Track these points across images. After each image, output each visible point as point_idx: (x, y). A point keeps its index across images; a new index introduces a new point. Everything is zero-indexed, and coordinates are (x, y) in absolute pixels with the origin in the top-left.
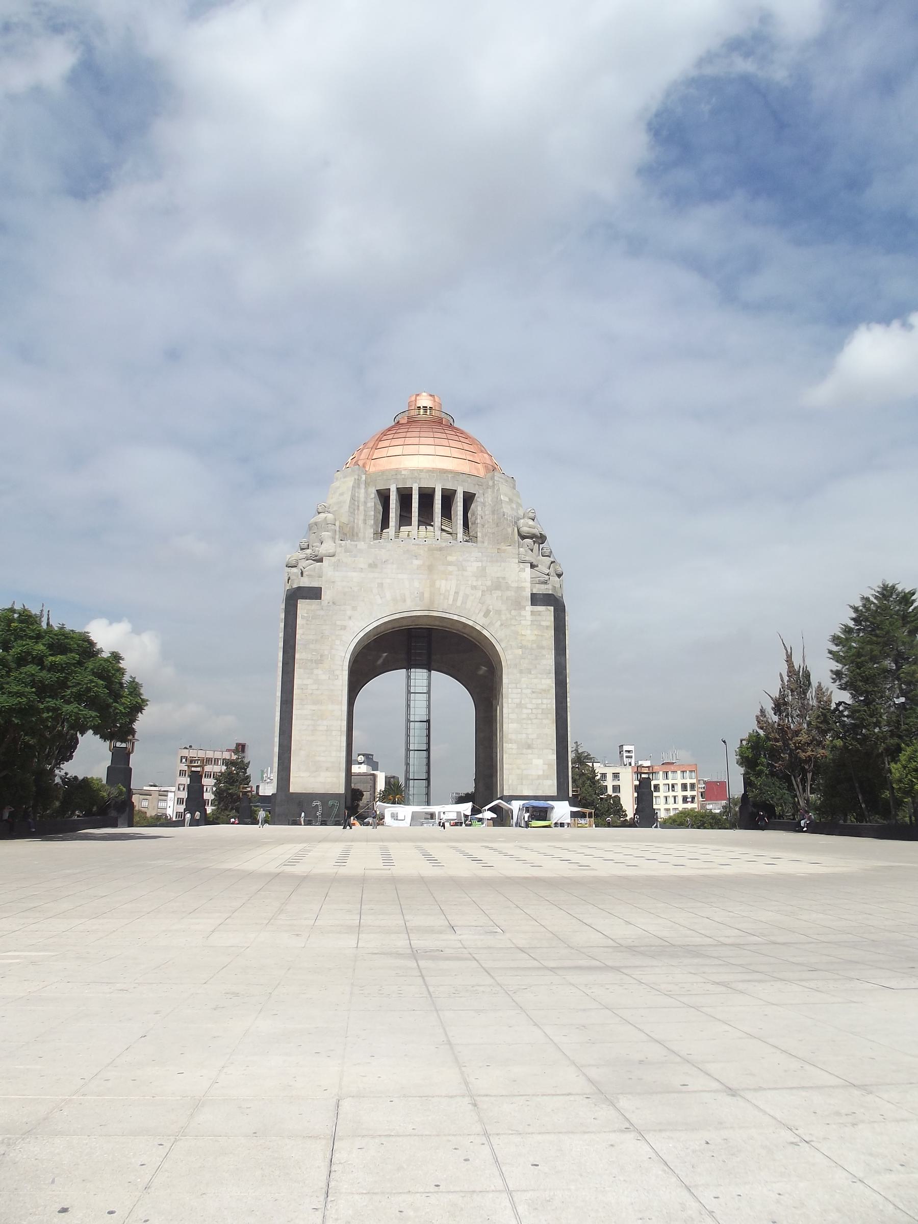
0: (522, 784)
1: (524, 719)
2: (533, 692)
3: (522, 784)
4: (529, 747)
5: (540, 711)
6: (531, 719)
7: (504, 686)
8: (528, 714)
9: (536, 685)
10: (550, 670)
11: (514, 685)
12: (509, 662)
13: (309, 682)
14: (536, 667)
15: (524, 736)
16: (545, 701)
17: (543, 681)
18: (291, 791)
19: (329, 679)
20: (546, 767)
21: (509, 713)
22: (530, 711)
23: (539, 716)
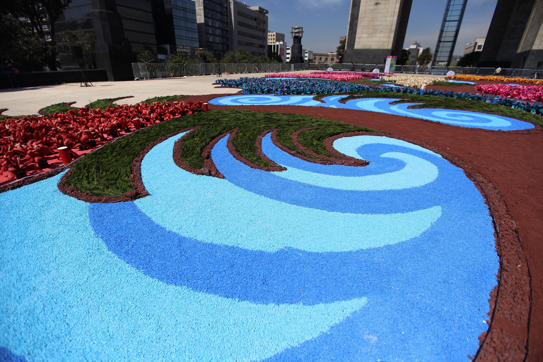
18: (356, 47)
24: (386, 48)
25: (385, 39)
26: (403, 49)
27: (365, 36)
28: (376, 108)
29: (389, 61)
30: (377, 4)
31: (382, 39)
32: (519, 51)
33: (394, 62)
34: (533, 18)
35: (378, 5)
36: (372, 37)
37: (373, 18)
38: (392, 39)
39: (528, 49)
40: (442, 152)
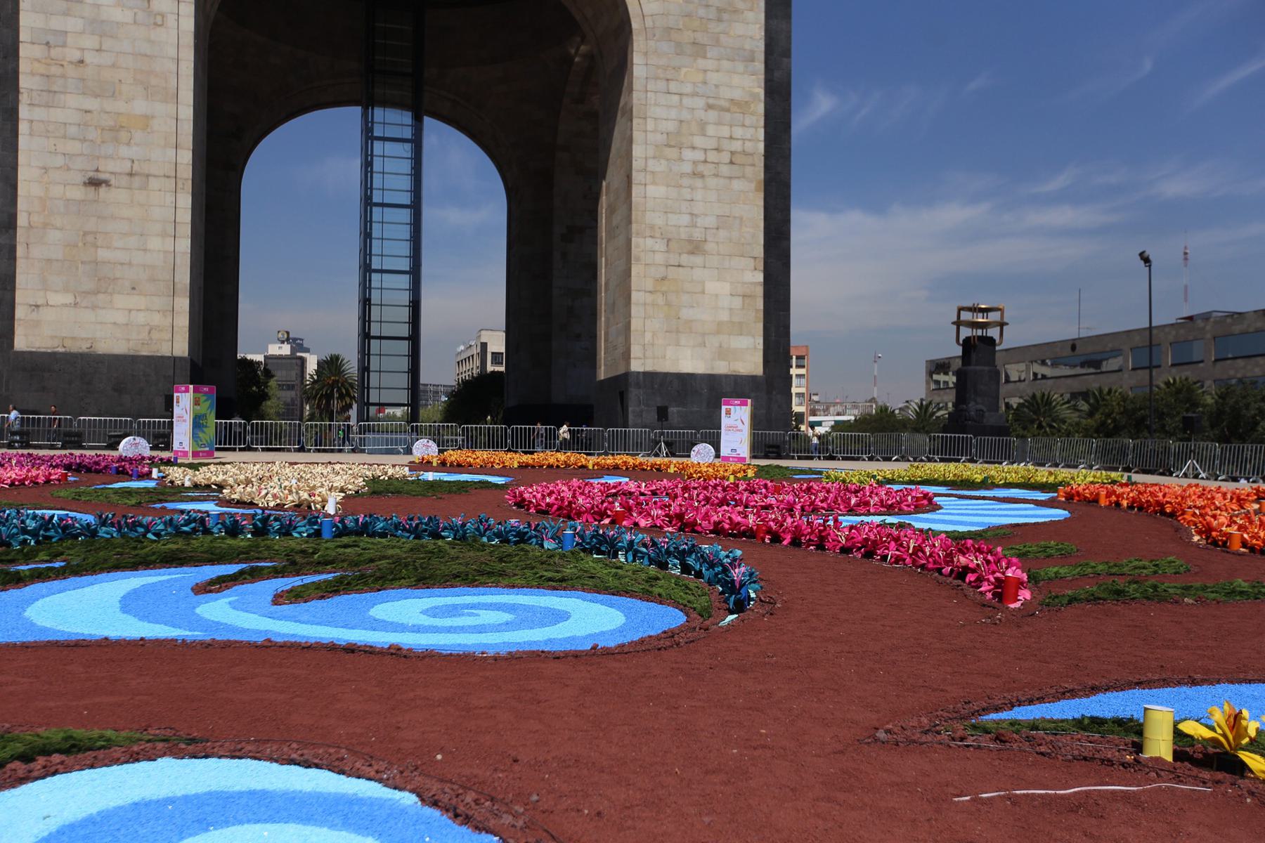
0: (678, 344)
1: (682, 175)
2: (710, 107)
3: (678, 344)
4: (696, 248)
5: (726, 157)
6: (703, 176)
7: (637, 85)
8: (695, 163)
9: (717, 86)
10: (752, 52)
11: (661, 85)
12: (649, 23)
13: (73, 24)
14: (718, 40)
15: (685, 219)
16: (738, 132)
17: (736, 80)
19: (135, 22)
20: (737, 302)
21: (646, 158)
22: (699, 156)
23: (725, 170)
24: (165, 351)
25: (157, 319)
26: (240, 356)
27: (56, 299)
28: (131, 620)
29: (185, 403)
30: (95, 183)
31: (141, 318)
32: (602, 374)
33: (208, 407)
34: (606, 284)
35: (103, 189)
36: (94, 307)
37: (85, 234)
38: (183, 321)
39: (621, 371)
40: (418, 780)
